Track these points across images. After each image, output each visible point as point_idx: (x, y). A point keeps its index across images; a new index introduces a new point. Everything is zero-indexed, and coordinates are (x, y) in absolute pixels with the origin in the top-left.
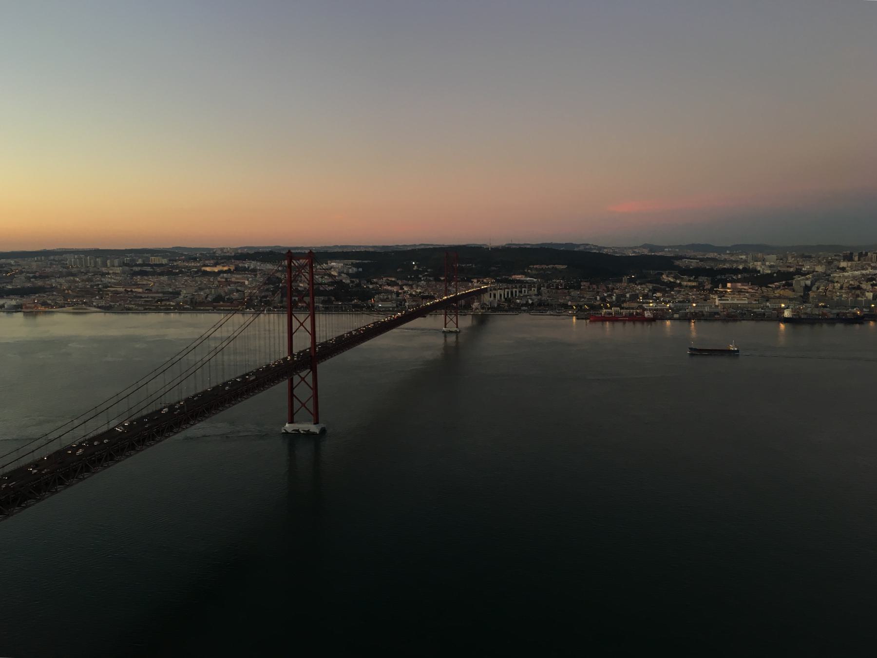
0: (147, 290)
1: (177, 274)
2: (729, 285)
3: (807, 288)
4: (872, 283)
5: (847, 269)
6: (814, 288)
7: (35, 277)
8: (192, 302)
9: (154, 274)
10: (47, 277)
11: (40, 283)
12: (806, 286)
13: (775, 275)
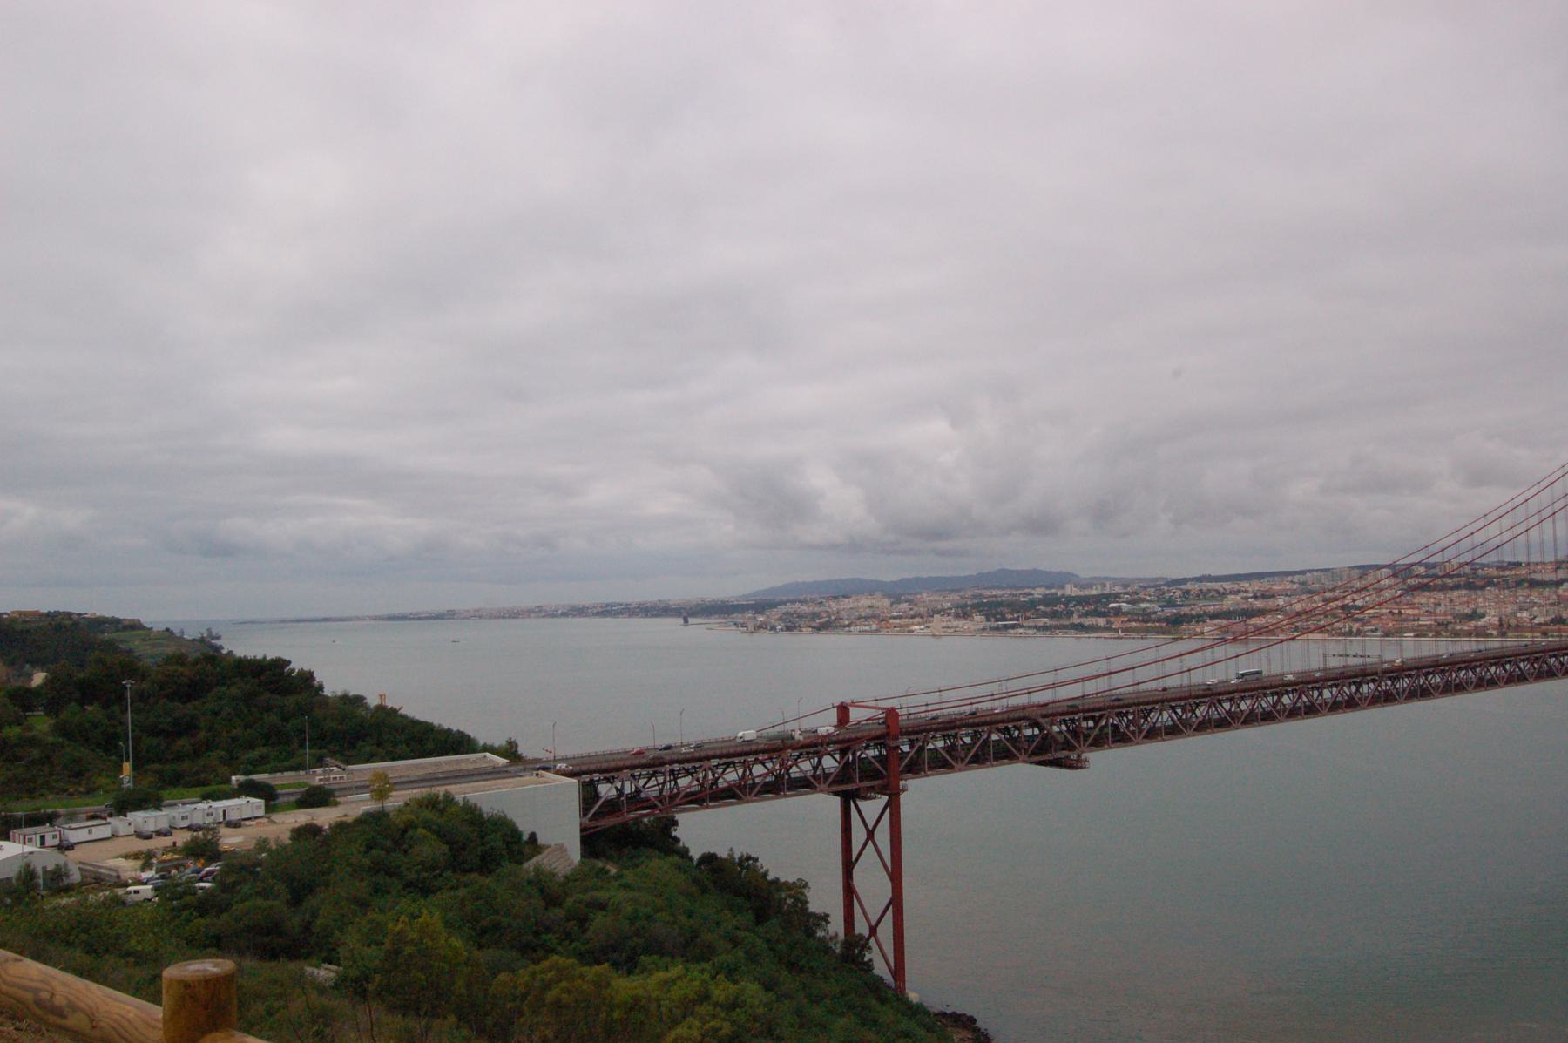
0: (1427, 611)
1: (1482, 588)
7: (1255, 597)
8: (1501, 625)
9: (1444, 588)
10: (1273, 596)
11: (1259, 604)
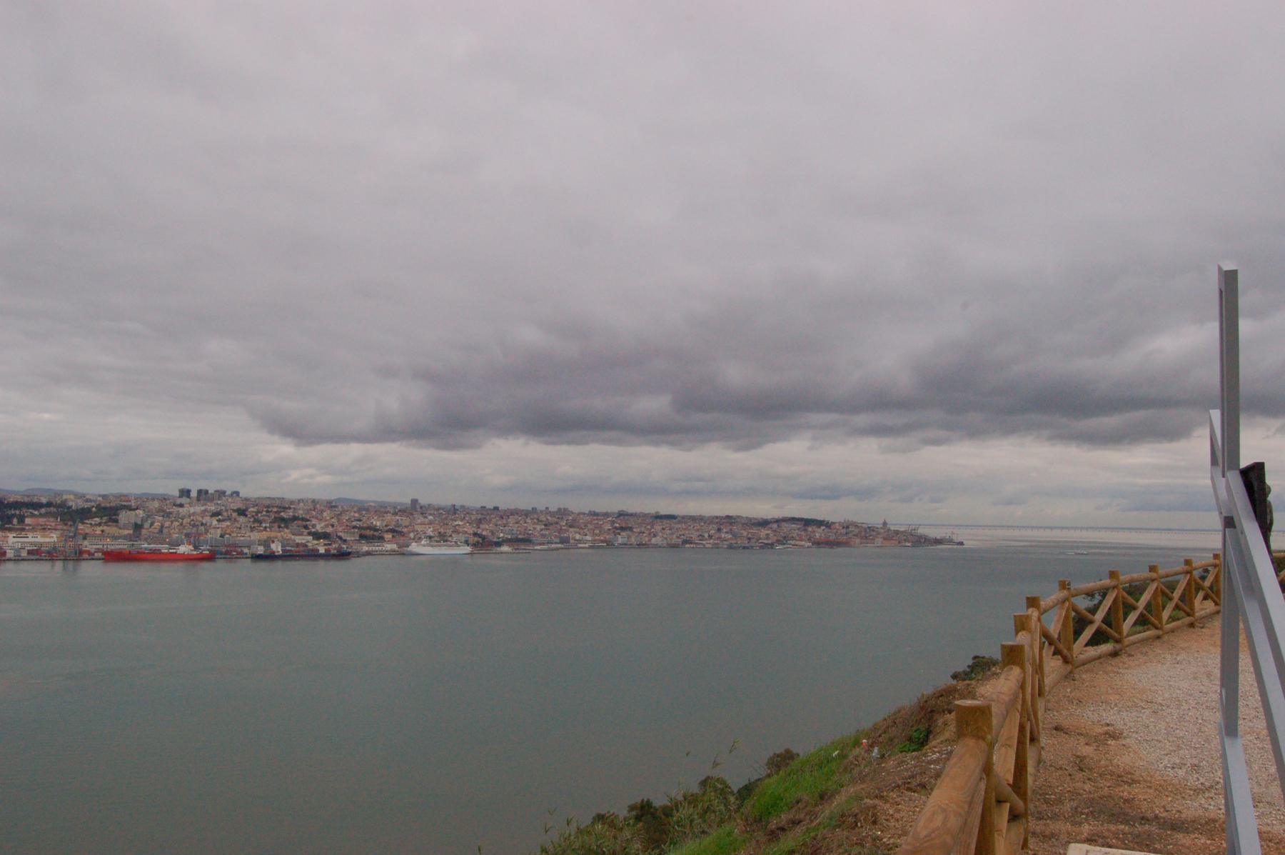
2: (28, 521)
3: (138, 527)
4: (217, 518)
5: (185, 505)
6: (147, 525)
12: (136, 524)
13: (94, 509)
